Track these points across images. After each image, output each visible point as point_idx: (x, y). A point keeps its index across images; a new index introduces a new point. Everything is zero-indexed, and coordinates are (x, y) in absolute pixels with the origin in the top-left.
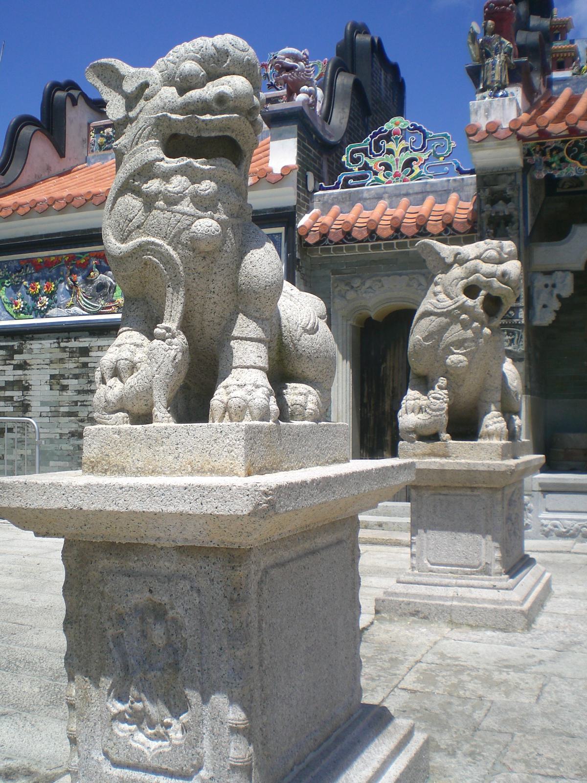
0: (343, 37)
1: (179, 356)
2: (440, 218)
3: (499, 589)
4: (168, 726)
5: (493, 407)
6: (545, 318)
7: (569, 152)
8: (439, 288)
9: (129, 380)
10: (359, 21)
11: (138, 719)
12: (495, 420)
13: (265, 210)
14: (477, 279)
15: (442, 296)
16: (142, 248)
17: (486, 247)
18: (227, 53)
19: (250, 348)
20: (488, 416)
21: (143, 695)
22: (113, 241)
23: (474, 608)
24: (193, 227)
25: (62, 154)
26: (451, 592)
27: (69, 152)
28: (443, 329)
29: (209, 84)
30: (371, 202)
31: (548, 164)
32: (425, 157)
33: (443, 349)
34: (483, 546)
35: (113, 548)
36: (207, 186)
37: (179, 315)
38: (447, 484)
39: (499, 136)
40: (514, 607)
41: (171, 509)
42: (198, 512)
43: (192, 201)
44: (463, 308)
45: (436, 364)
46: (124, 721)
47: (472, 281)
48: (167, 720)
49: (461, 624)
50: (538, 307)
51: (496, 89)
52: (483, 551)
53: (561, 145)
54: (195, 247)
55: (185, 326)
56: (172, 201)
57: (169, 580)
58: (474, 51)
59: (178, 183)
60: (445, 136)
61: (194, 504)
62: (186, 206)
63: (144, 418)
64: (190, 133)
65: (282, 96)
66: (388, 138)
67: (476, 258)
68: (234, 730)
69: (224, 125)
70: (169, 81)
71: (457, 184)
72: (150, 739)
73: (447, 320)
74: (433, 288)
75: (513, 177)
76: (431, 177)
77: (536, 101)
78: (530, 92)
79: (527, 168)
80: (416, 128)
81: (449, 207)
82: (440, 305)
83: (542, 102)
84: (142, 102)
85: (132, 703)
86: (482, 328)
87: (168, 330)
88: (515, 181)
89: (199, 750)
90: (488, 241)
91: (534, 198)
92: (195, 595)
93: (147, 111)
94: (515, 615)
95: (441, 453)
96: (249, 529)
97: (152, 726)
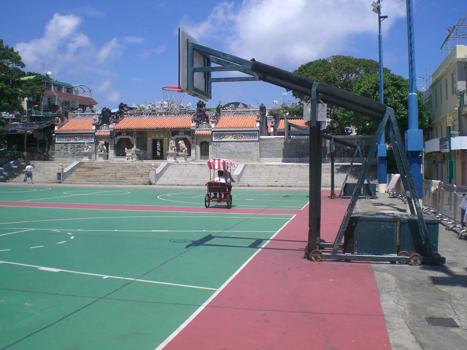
6: (116, 143)
25: (68, 119)
27: (69, 119)
30: (102, 132)
66: (104, 126)
79: (114, 131)
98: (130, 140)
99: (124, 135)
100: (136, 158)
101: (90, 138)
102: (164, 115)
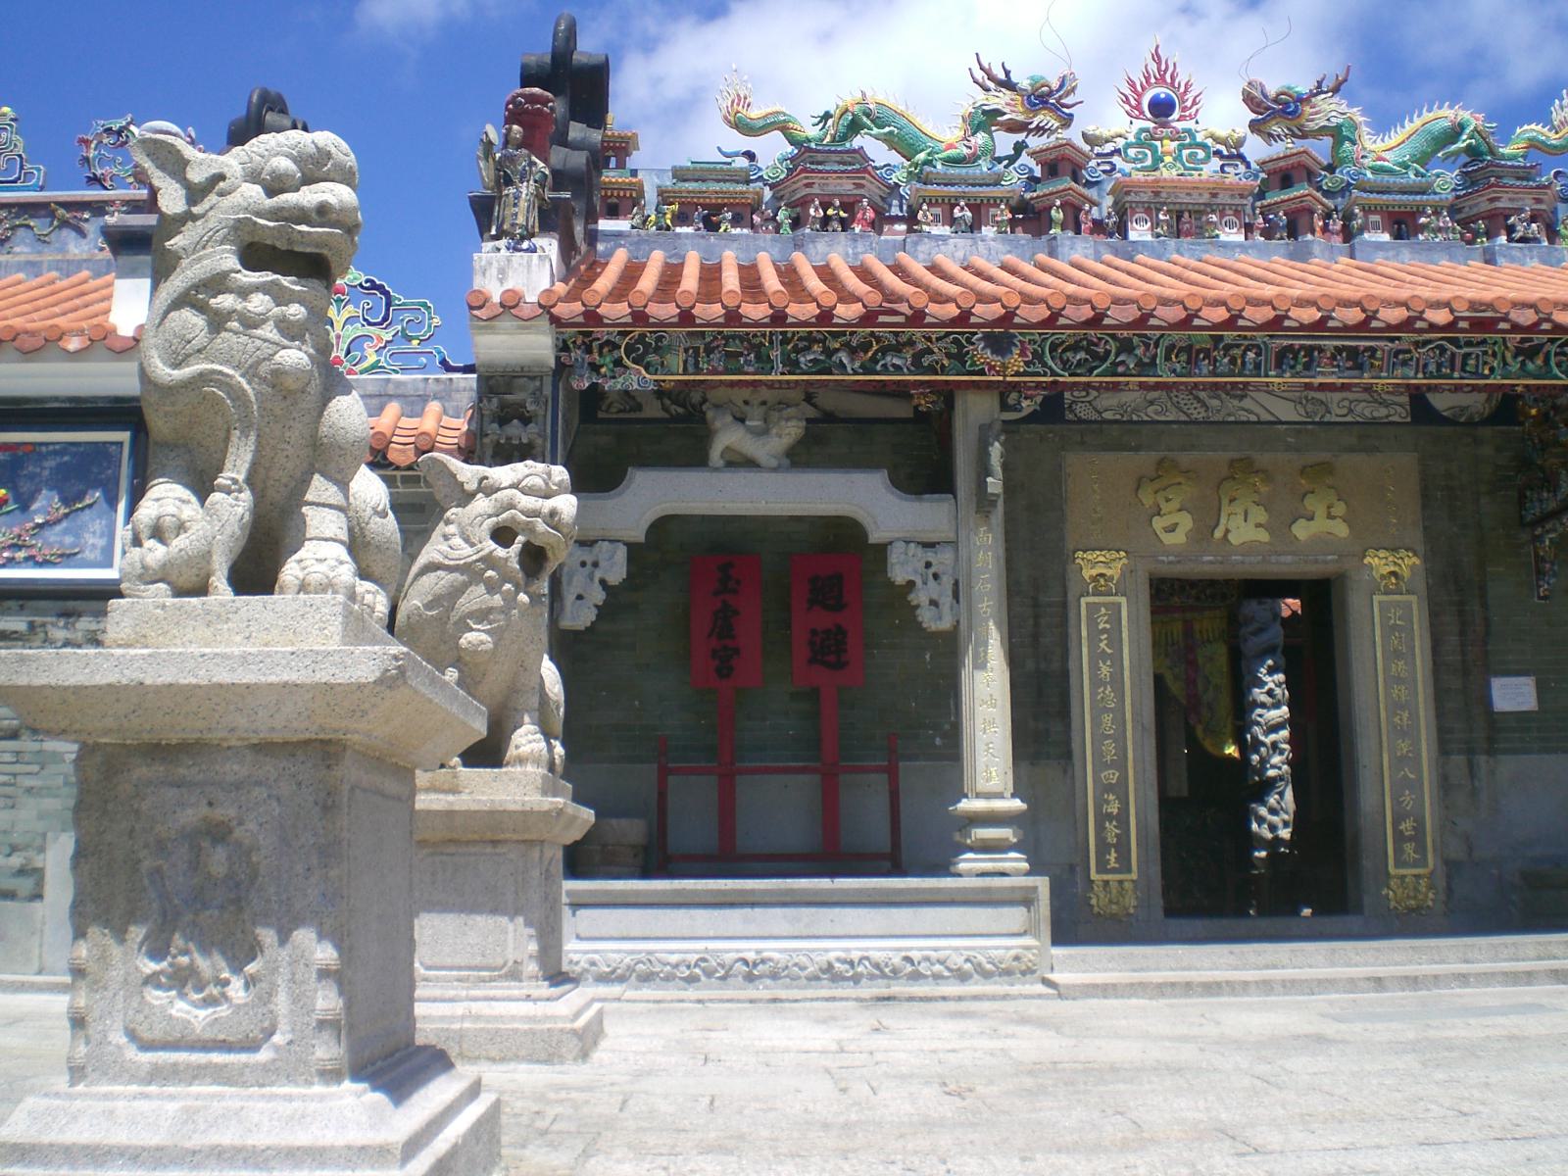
0: (243, 112)
1: (247, 517)
2: (412, 440)
3: (536, 1000)
4: (226, 983)
5: (527, 719)
6: (580, 616)
7: (629, 350)
8: (452, 529)
9: (175, 542)
10: (273, 89)
11: (181, 980)
12: (531, 737)
13: (95, 399)
14: (513, 518)
15: (457, 541)
16: (203, 377)
17: (527, 471)
18: (329, 155)
19: (329, 517)
20: (520, 731)
21: (191, 945)
22: (160, 365)
23: (497, 1031)
24: (277, 357)
26: (459, 1009)
28: (457, 591)
29: (304, 188)
31: (595, 368)
32: (387, 336)
33: (455, 623)
34: (511, 935)
35: (158, 751)
36: (296, 311)
37: (247, 465)
38: (455, 836)
39: (520, 314)
40: (560, 1025)
41: (273, 679)
42: (308, 681)
43: (276, 326)
44: (489, 561)
45: (443, 647)
46: (159, 986)
47: (504, 521)
48: (225, 975)
49: (478, 1058)
50: (569, 598)
51: (519, 239)
52: (511, 944)
53: (617, 339)
54: (277, 381)
55: (254, 480)
56: (250, 323)
57: (238, 788)
58: (486, 171)
59: (259, 303)
60: (425, 305)
61: (303, 672)
62: (268, 331)
63: (201, 590)
64: (278, 244)
65: (113, 202)
67: (511, 486)
68: (324, 974)
69: (321, 241)
70: (254, 177)
71: (442, 387)
72: (196, 1007)
73: (465, 577)
74: (441, 528)
75: (538, 383)
76: (396, 372)
77: (579, 264)
78: (568, 249)
79: (561, 369)
80: (374, 286)
81: (428, 423)
82: (455, 554)
83: (583, 267)
84: (213, 198)
85: (174, 957)
86: (517, 593)
87: (235, 481)
88: (540, 389)
89: (272, 1007)
90: (529, 462)
91: (566, 421)
92: (275, 804)
93: (221, 210)
94: (564, 1037)
95: (446, 787)
96: (367, 706)
97: (200, 989)
98: (882, 549)
99: (750, 464)
100: (1026, 900)
101: (46, 504)
102: (1233, 236)
